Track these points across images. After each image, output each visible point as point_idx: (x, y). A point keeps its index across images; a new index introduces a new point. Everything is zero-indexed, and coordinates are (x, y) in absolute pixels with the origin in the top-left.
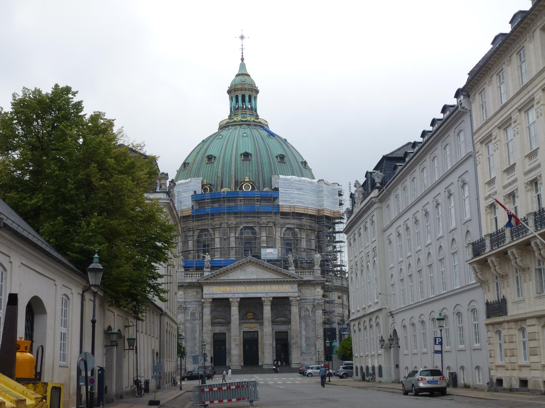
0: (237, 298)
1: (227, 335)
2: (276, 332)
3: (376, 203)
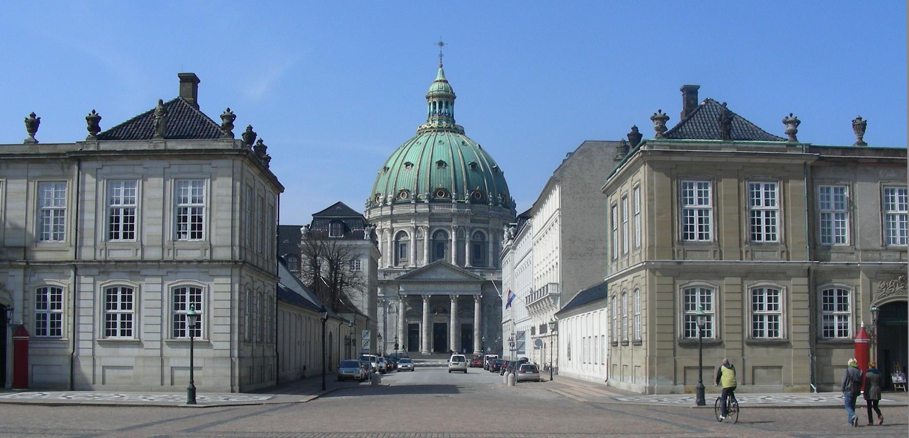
0: (428, 296)
1: (420, 325)
2: (462, 325)
3: (510, 249)
